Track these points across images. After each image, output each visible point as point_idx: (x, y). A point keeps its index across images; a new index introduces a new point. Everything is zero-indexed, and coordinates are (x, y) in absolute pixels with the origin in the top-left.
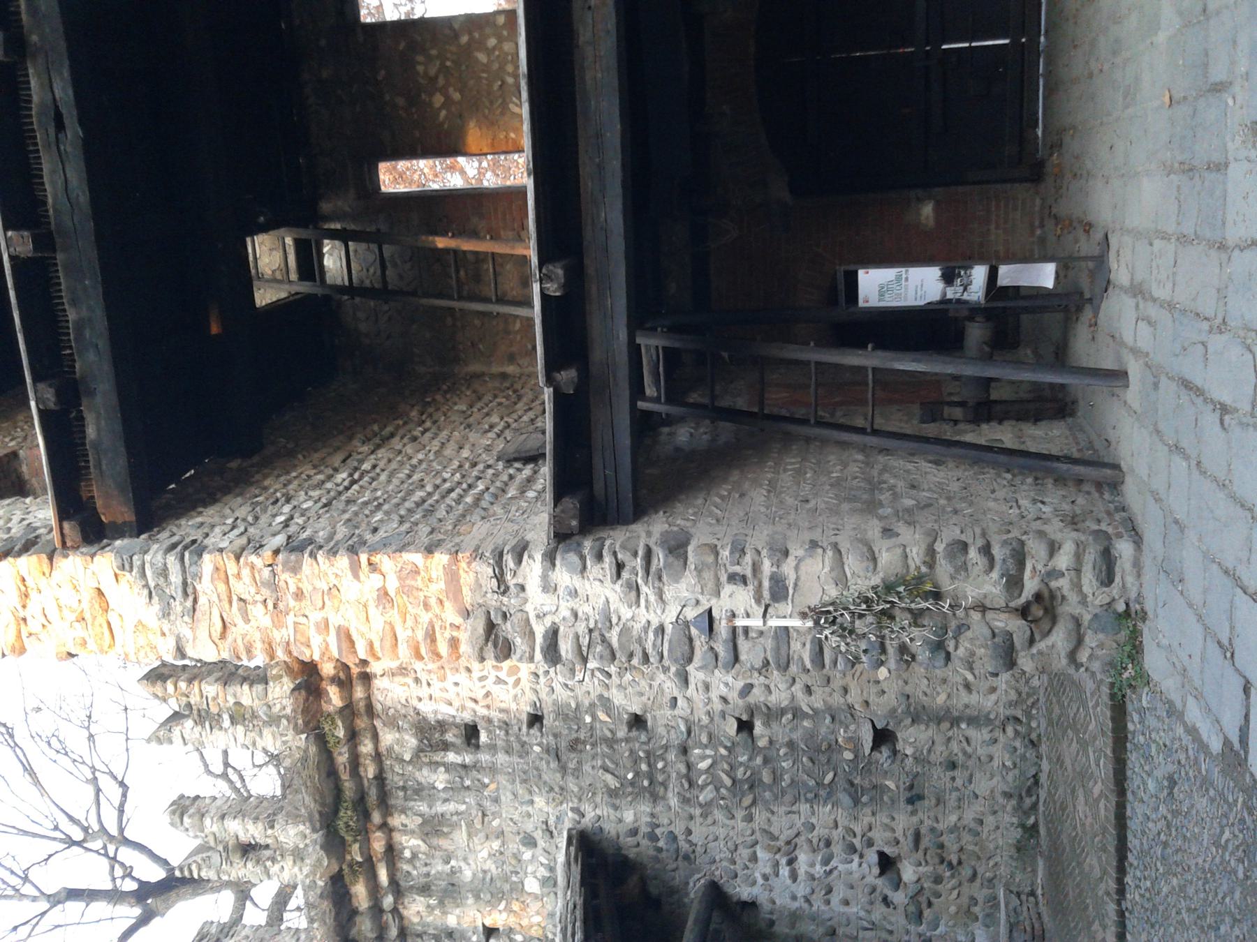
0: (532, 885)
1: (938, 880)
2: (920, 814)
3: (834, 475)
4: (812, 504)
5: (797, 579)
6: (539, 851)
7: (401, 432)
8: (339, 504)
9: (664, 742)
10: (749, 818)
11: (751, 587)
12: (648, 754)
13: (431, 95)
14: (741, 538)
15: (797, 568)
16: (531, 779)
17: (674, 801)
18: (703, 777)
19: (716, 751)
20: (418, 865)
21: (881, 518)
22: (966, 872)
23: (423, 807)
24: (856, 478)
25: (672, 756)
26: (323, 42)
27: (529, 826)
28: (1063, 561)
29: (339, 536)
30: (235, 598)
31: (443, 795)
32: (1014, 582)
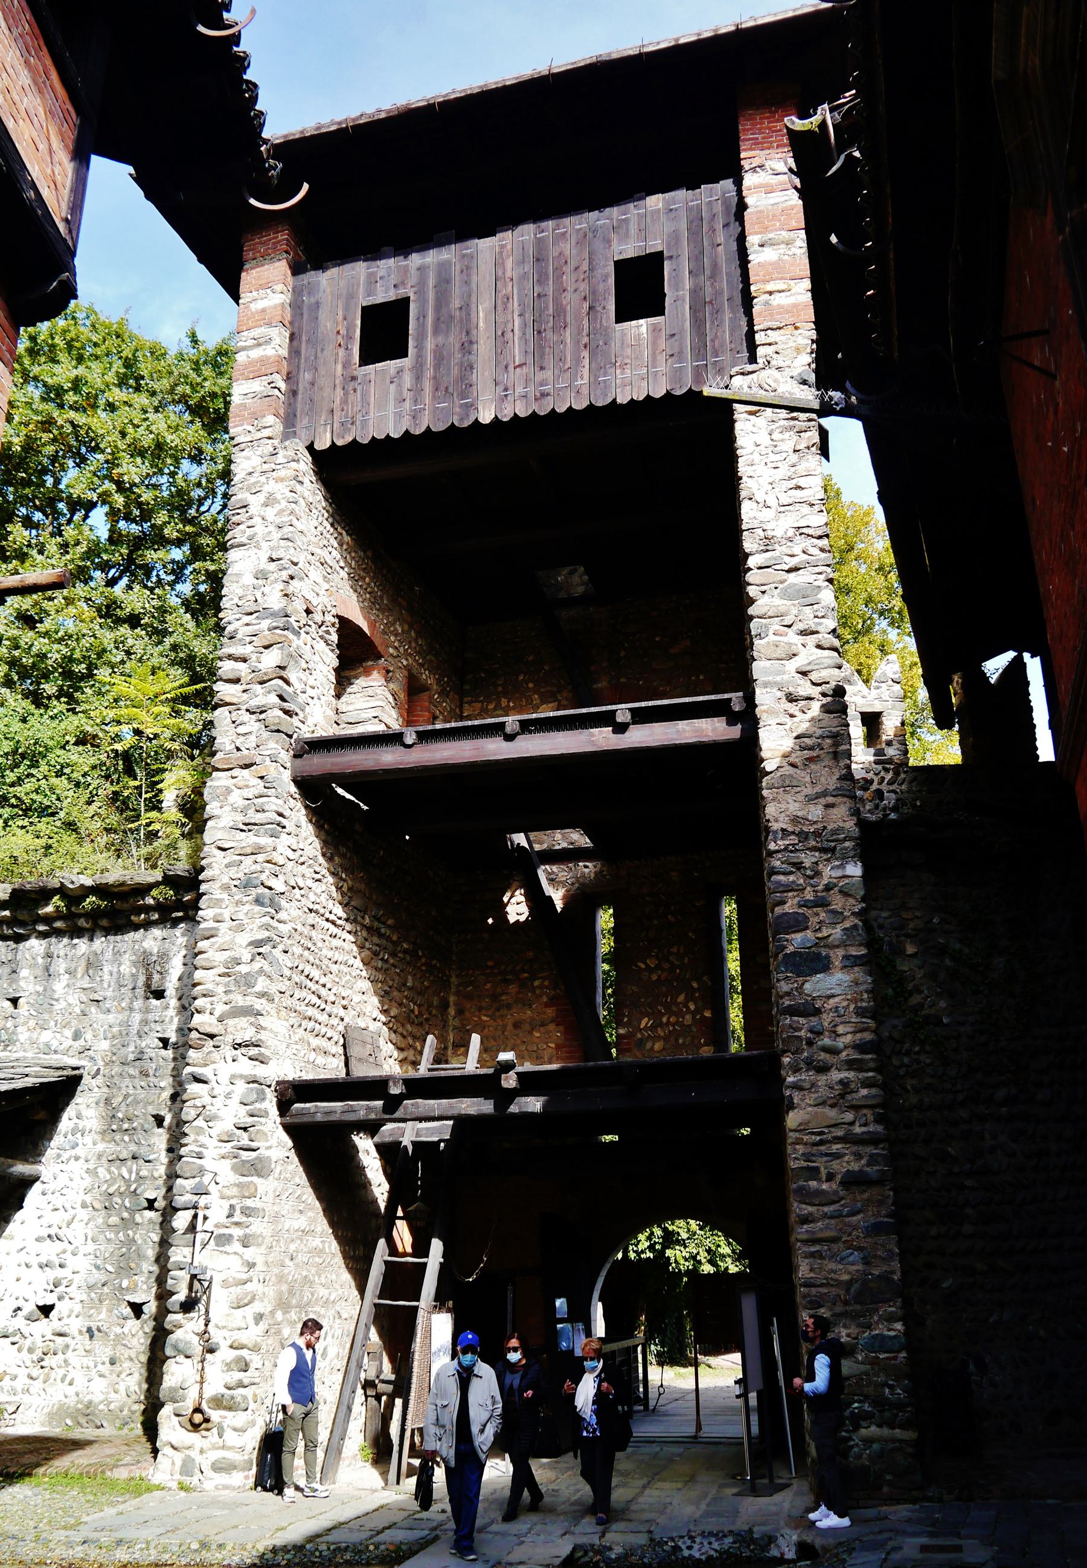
0: (46, 1036)
1: (31, 1351)
2: (79, 1337)
3: (316, 1278)
4: (288, 1262)
5: (228, 1254)
6: (71, 1042)
7: (384, 942)
8: (312, 918)
9: (143, 1142)
10: (84, 1205)
11: (226, 1220)
12: (134, 1129)
14: (261, 1214)
15: (235, 1253)
16: (121, 1037)
17: (101, 1147)
18: (116, 1172)
19: (135, 1182)
20: (68, 948)
21: (273, 1313)
22: (36, 1372)
24: (313, 1295)
25: (133, 1148)
27: (89, 1036)
28: (230, 1437)
29: (281, 926)
30: (243, 858)
31: (115, 970)
32: (218, 1402)
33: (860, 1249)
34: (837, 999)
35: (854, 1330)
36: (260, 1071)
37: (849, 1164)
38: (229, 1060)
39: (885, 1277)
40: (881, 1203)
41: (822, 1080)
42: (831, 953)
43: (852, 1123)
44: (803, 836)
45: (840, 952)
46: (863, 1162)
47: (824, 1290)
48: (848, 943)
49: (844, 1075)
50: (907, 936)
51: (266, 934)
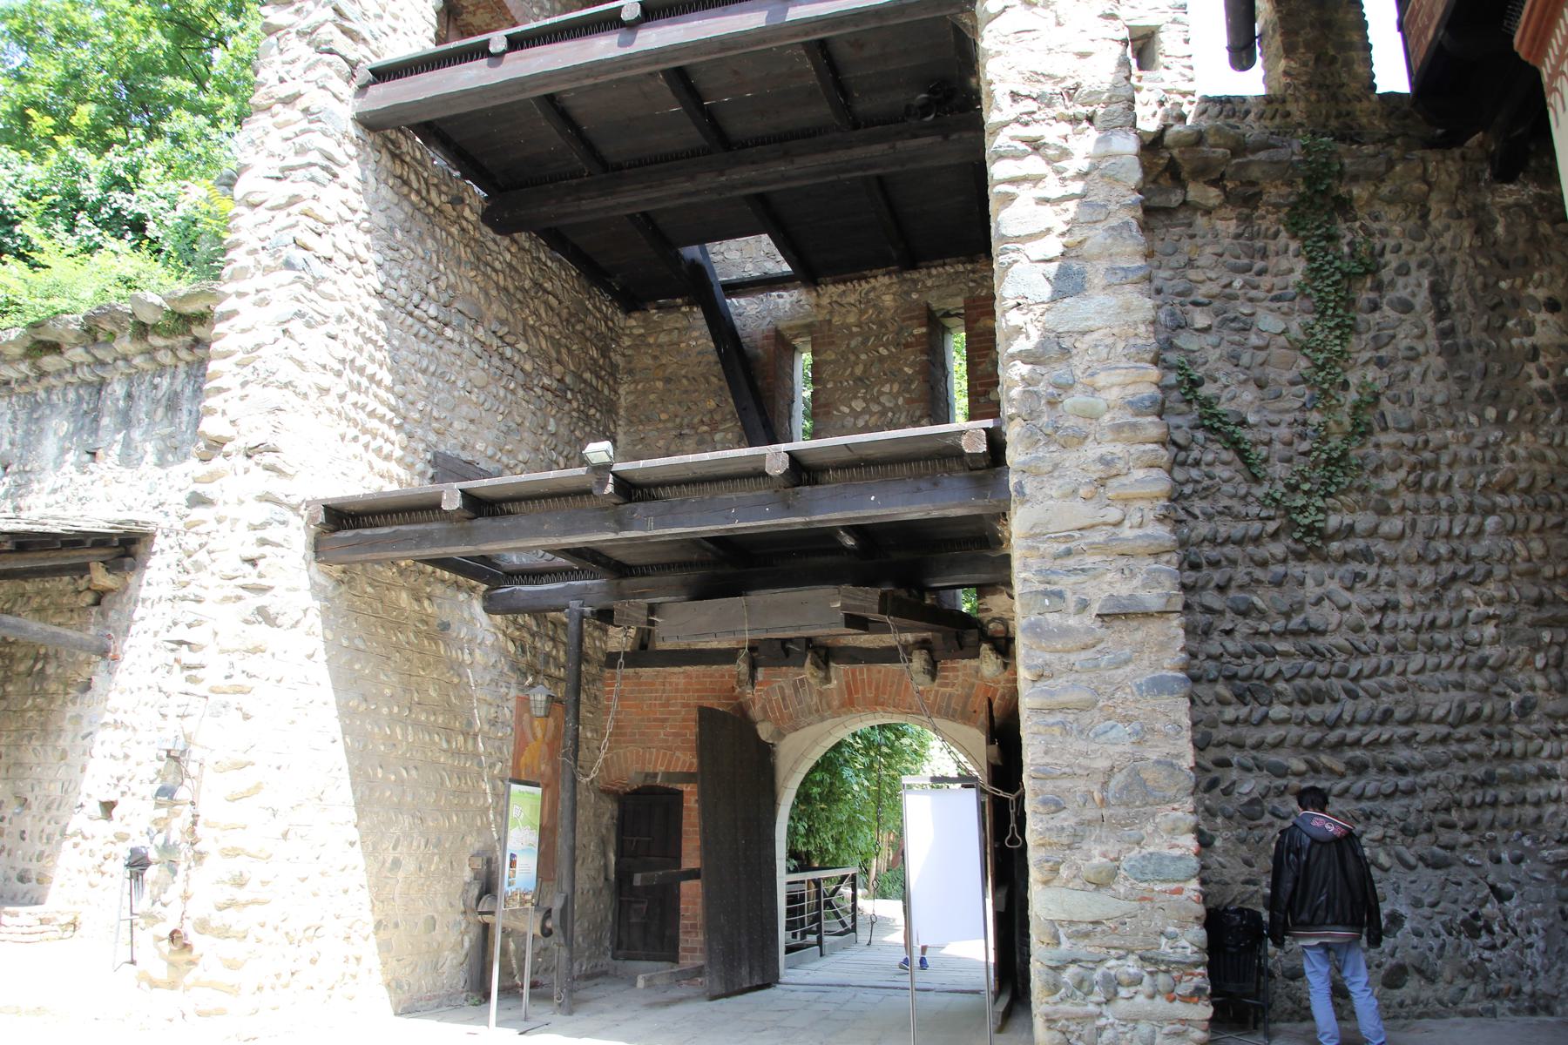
13: (864, 399)
23: (188, 392)
26: (915, 296)
33: (1127, 719)
34: (1096, 335)
35: (1113, 848)
36: (277, 486)
37: (1111, 586)
38: (240, 471)
39: (1168, 764)
40: (1163, 647)
41: (1071, 458)
42: (1088, 267)
43: (1118, 524)
44: (1045, 100)
45: (1103, 265)
46: (1136, 582)
47: (1066, 783)
48: (1114, 250)
49: (1105, 449)
50: (1196, 304)
51: (297, 306)
